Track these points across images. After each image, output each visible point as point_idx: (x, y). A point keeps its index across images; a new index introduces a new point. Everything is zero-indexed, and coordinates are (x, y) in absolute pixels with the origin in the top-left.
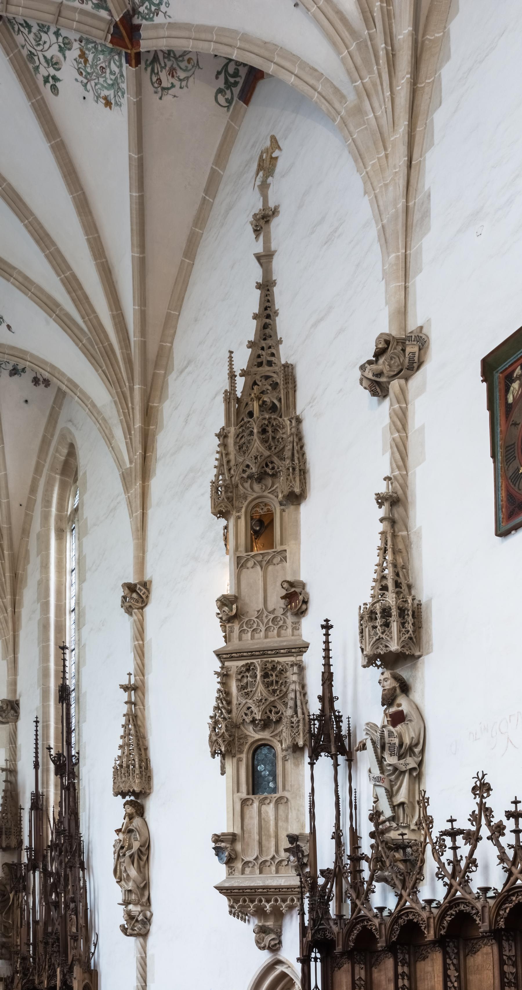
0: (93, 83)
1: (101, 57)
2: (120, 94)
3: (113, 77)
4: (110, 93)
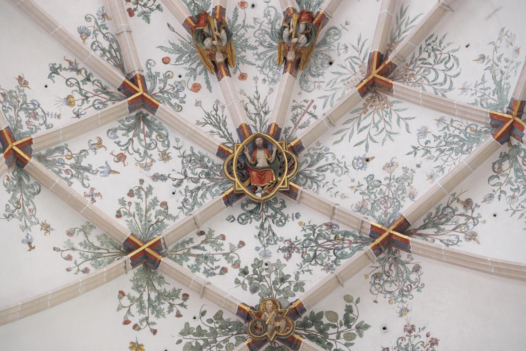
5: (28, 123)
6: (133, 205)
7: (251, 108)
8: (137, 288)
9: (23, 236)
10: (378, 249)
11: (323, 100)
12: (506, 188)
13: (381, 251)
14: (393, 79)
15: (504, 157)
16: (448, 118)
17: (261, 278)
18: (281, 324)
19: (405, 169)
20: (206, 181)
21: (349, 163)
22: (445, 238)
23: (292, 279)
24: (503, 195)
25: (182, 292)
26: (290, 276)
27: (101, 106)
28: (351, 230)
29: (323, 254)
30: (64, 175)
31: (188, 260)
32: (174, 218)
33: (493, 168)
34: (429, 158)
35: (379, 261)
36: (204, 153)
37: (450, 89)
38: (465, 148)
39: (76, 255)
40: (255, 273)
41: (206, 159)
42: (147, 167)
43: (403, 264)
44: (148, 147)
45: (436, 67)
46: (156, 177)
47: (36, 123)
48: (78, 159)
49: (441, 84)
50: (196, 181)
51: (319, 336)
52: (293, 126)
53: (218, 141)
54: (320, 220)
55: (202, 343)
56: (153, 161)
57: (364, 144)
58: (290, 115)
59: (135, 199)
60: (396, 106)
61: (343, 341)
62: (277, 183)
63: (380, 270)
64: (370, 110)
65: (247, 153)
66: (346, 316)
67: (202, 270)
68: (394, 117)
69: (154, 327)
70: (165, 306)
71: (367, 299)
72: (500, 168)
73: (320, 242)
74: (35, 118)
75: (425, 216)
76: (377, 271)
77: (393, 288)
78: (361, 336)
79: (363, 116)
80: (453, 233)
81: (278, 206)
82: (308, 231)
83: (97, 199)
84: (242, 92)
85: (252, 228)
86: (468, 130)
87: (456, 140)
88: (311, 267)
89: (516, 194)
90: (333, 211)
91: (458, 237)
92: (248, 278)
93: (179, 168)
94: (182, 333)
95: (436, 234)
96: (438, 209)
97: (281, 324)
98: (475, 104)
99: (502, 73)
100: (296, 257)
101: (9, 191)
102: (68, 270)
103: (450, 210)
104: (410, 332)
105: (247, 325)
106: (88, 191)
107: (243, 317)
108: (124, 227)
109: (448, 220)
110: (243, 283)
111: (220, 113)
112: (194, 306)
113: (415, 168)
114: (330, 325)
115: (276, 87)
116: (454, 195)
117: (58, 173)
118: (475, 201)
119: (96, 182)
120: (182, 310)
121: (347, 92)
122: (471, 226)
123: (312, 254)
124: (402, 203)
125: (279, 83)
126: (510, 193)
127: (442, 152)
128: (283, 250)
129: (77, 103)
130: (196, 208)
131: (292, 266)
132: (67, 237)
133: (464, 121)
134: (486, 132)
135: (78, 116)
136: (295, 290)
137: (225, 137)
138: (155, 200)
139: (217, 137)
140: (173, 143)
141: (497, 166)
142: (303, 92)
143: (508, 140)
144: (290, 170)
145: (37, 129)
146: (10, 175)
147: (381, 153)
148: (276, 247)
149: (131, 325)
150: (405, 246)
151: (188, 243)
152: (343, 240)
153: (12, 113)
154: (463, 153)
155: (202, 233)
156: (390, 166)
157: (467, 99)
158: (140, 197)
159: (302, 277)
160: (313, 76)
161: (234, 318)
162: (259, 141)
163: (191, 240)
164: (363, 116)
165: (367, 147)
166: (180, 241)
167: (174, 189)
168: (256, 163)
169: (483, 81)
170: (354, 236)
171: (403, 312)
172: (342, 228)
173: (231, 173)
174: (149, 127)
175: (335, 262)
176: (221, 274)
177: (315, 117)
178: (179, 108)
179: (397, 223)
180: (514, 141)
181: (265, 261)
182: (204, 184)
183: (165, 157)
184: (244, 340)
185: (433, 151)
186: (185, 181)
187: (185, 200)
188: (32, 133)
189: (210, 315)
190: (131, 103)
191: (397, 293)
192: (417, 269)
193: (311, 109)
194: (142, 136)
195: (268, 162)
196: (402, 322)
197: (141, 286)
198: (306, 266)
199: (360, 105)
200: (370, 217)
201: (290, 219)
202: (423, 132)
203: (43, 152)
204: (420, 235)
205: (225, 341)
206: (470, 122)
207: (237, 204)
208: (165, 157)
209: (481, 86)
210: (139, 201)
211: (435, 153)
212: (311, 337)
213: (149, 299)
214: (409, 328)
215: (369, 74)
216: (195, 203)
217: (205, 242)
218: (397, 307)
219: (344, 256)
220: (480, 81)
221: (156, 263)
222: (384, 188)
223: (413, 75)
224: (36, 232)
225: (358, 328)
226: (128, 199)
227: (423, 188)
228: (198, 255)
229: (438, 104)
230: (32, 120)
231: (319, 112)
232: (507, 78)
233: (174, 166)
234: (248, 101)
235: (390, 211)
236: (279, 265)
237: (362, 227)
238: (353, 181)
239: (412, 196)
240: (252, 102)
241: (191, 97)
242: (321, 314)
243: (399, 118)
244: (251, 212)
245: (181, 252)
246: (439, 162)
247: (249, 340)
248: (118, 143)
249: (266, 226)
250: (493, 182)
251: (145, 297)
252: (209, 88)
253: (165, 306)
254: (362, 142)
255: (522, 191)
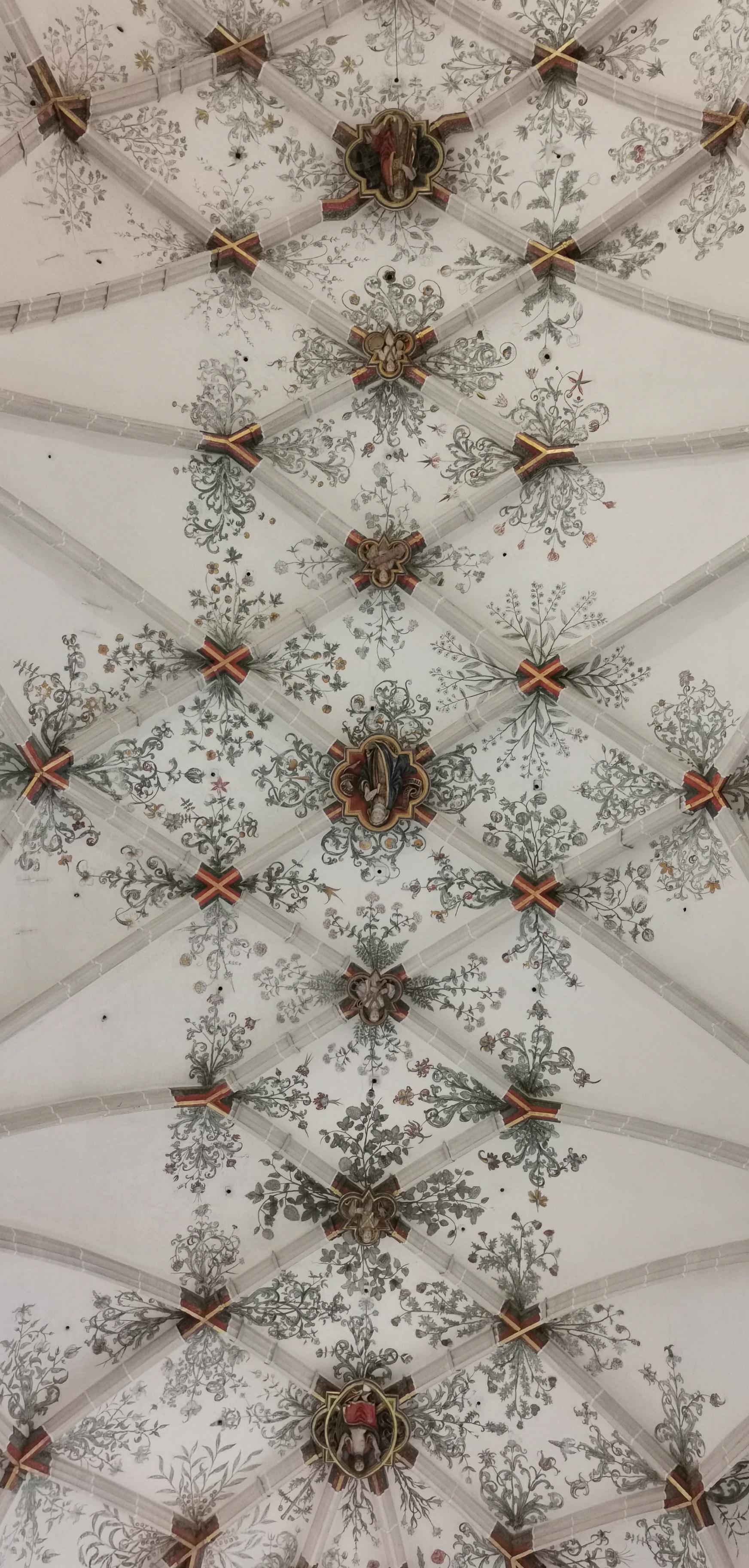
0: (688, 884)
1: (686, 848)
2: (723, 861)
3: (707, 854)
4: (713, 874)
5: (671, 1532)
6: (533, 1393)
7: (366, 1518)
8: (534, 1278)
9: (680, 1368)
10: (222, 1296)
11: (269, 1517)
12: (46, 1364)
13: (219, 1293)
14: (171, 1539)
15: (41, 1409)
16: (106, 1473)
17: (375, 1272)
18: (355, 1211)
19: (172, 1404)
20: (434, 1416)
21: (245, 1420)
22: (136, 1304)
23: (336, 1268)
24: (53, 1355)
25: (476, 1265)
26: (339, 1272)
27: (570, 1545)
28: (254, 1326)
29: (292, 1298)
30: (623, 1448)
31: (467, 1308)
32: (480, 1367)
33: (58, 1394)
34: (139, 1417)
35: (223, 1281)
36: (434, 1458)
37: (96, 1516)
38: (90, 1427)
39: (612, 1332)
40: (382, 1281)
41: (433, 1447)
42: (512, 1446)
43: (193, 1274)
44: (509, 1475)
45: (111, 1551)
46: (500, 1429)
47: (659, 1531)
48: (603, 1468)
49: (107, 1524)
50: (447, 1417)
51: (310, 1190)
52: (313, 1484)
53: (414, 1473)
54: (292, 1345)
55: (457, 1196)
56: (504, 1454)
57: (221, 1446)
58: (315, 1501)
59: (531, 1401)
60: (172, 1497)
61: (281, 1180)
62: (342, 1403)
63: (224, 1268)
64: (207, 1495)
65: (377, 1451)
66: (274, 1211)
67: (449, 1292)
68: (176, 1482)
69: (515, 1223)
70: (499, 1249)
71: (245, 1232)
72: (50, 1394)
73: (295, 1314)
74: (660, 1537)
75: (157, 1335)
76: (228, 1267)
77: (212, 1243)
78: (259, 1185)
79: (217, 1488)
80: (124, 1309)
81: (344, 1370)
82: (308, 1330)
83: (581, 1408)
84: (377, 1543)
85: (380, 1343)
86: (81, 1452)
87: (99, 1440)
88: (311, 1281)
89: (34, 1355)
90: (275, 1355)
91: (120, 1303)
92: (391, 1274)
93: (469, 1439)
94: (480, 1211)
95: (145, 1310)
96: (138, 1344)
97: (355, 1211)
98: (66, 1490)
99: (23, 1533)
100: (327, 1296)
101: (698, 1435)
102: (621, 1312)
103: (124, 1341)
104: (198, 1184)
105: (398, 1213)
106: (592, 1420)
107: (403, 1224)
108: (546, 1362)
109: (128, 1327)
110: (398, 1266)
111: (409, 1515)
112: (462, 1246)
113: (160, 1405)
114: (296, 1203)
115: (329, 1545)
116: (115, 1361)
117: (631, 1452)
118: (89, 1350)
119: (581, 1433)
120: (479, 1241)
121: (235, 1526)
122: (100, 1317)
123: (307, 1299)
124: (183, 1357)
125: (325, 1551)
126: (43, 1357)
127: (121, 1425)
128: (343, 1308)
129: (603, 1554)
130: (451, 1379)
131: (334, 1286)
132: (622, 1357)
133: (85, 1466)
134: (59, 1447)
135: (602, 1534)
136: (333, 1252)
137: (405, 1478)
138: (504, 1395)
139: (415, 1479)
140: (475, 1476)
141: (54, 1396)
142: (294, 1533)
143: (32, 1432)
144: (322, 1420)
145: (658, 1521)
146: (695, 1458)
147: (200, 1431)
148: (352, 1313)
149: (544, 1228)
150: (187, 1298)
151: (465, 1332)
152: (265, 1314)
153: (693, 1551)
154: (94, 1420)
155: (446, 1343)
156: (192, 1411)
157: (76, 1498)
158: (524, 1404)
159: (323, 1268)
160: (277, 1556)
161: (413, 1224)
162: (359, 1467)
163: (460, 1334)
164: (217, 1488)
165: (218, 1442)
166: (475, 1334)
167: (478, 1410)
168: (365, 1435)
169: (50, 1523)
170: (251, 1318)
171: (202, 1210)
172: (264, 1330)
173: (401, 1424)
174: (506, 1505)
175: (279, 1285)
176: (425, 1284)
177: (282, 1494)
178: (465, 1529)
179: (193, 1330)
180: (24, 1430)
181: (367, 1295)
182: (438, 1411)
183: (487, 1458)
184: (403, 1195)
185: (133, 1427)
186: (462, 1420)
187: (464, 1391)
188: (666, 1516)
189: (443, 1231)
190: (529, 1546)
191: (207, 1236)
192: (177, 1265)
193: (286, 1506)
194: (516, 1493)
195: (350, 1434)
196: (206, 1198)
197: (528, 1279)
198: (315, 1283)
199: (219, 1504)
200: (227, 1341)
201: (330, 1350)
202: (141, 1455)
203: (650, 1485)
204: (166, 1310)
205: (427, 1195)
206: (78, 1463)
207: (397, 1379)
208: (487, 1458)
209: (55, 1514)
210: (525, 1398)
211: (131, 1424)
212: (320, 1189)
213: (519, 1261)
214: (198, 1189)
215: (201, 1552)
216: (452, 1386)
217: (443, 1330)
218: (210, 1218)
219: (267, 1291)
220: (55, 1522)
221: (508, 1308)
222: (204, 1380)
223: (143, 1542)
224: (662, 1371)
225: (261, 1195)
226: (540, 1402)
227: (152, 1376)
228: (453, 1312)
229: (116, 1495)
230: (666, 1536)
231: (276, 1500)
232: (18, 1523)
233: (476, 1442)
234: (369, 1528)
235: (200, 1348)
236: (351, 1288)
237: (239, 1329)
238: (243, 1395)
239: (169, 1365)
240: (364, 1525)
241: (446, 1543)
242: (305, 1217)
243: (170, 1480)
244: (379, 1365)
245: (475, 1319)
246: (127, 1409)
247: (397, 1193)
248: (549, 1486)
249: (362, 1344)
250: (62, 1374)
251: (524, 1263)
252: (420, 1555)
253: (499, 1249)
254: (224, 1449)
255: (27, 1359)
